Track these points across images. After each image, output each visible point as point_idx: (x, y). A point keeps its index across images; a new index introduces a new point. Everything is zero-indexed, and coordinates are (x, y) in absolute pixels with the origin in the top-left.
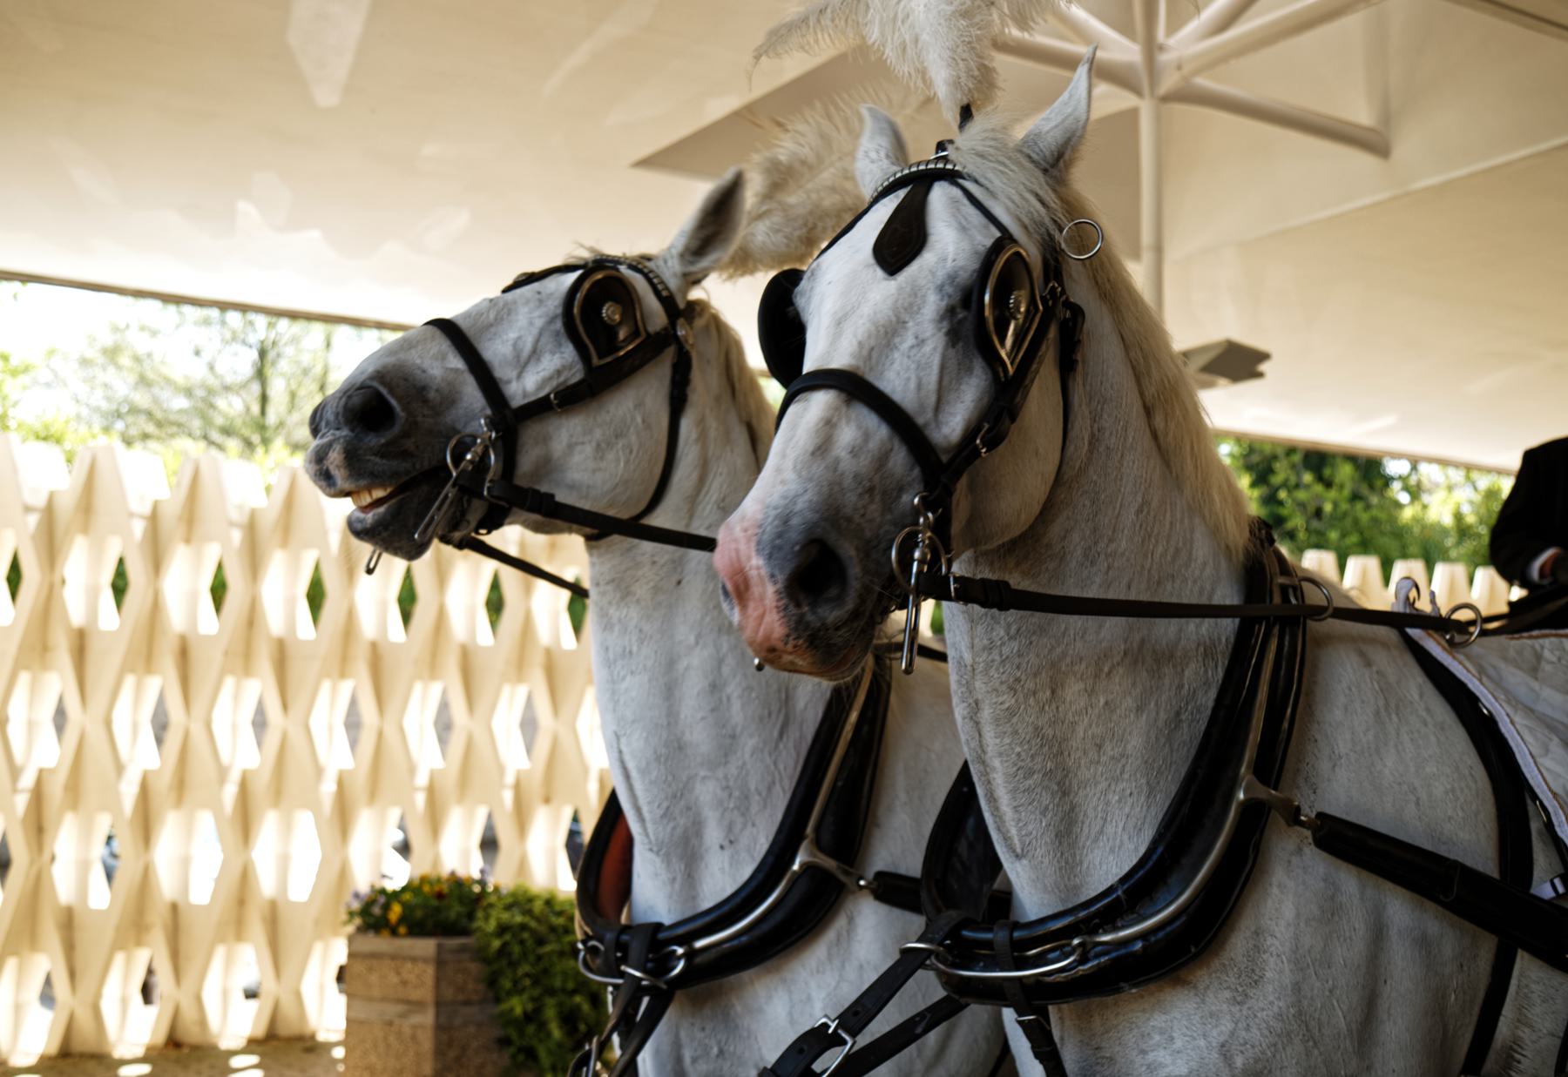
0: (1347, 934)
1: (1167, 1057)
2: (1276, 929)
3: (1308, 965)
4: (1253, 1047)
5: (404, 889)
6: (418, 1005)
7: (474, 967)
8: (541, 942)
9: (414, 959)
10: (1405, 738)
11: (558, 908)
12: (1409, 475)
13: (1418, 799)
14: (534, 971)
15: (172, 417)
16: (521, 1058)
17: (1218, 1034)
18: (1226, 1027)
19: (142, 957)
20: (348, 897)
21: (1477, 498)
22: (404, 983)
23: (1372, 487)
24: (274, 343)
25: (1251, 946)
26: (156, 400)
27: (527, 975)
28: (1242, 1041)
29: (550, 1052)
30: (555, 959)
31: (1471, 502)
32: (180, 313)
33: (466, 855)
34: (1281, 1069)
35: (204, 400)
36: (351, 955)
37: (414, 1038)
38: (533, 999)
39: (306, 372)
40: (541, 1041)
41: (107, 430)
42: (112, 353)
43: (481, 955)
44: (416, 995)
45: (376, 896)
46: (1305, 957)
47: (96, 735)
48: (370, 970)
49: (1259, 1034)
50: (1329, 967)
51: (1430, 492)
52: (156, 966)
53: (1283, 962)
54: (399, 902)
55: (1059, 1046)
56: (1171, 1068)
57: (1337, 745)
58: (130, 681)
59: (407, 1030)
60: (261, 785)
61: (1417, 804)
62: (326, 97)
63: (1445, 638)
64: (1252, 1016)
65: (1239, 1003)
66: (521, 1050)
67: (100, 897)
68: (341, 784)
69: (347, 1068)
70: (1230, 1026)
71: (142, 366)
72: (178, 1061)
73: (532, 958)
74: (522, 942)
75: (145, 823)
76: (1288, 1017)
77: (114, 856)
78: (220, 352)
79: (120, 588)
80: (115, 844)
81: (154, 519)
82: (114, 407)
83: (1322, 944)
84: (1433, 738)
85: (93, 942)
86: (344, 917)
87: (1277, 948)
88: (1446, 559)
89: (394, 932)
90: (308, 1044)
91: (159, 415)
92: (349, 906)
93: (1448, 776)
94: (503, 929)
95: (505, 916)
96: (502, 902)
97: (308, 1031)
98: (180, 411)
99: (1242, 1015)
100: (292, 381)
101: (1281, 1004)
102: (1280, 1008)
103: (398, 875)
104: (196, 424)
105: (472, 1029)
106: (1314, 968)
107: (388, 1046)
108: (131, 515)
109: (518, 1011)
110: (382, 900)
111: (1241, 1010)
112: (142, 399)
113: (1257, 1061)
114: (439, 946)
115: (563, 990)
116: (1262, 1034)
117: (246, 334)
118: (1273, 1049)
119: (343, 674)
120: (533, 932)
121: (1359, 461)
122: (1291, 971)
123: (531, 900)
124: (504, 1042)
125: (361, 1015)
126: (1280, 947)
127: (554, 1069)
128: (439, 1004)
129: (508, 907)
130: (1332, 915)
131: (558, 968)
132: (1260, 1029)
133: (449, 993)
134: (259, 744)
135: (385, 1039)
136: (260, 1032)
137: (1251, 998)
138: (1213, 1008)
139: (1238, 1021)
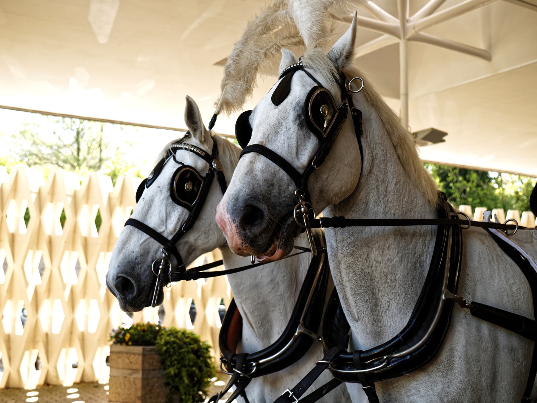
5: (131, 328)
6: (135, 371)
7: (156, 357)
8: (181, 348)
9: (134, 354)
11: (187, 336)
12: (498, 178)
15: (45, 156)
16: (173, 390)
19: (35, 353)
20: (110, 331)
21: (523, 186)
22: (131, 362)
23: (484, 182)
26: (39, 151)
27: (176, 360)
29: (184, 387)
30: (186, 354)
31: (520, 188)
32: (48, 118)
35: (56, 150)
36: (111, 352)
37: (134, 382)
38: (178, 369)
40: (180, 384)
41: (21, 161)
42: (23, 133)
43: (159, 352)
44: (135, 367)
47: (18, 272)
48: (119, 357)
51: (505, 184)
52: (40, 356)
54: (129, 333)
58: (31, 252)
59: (132, 380)
62: (103, 39)
66: (173, 387)
67: (20, 331)
71: (34, 137)
72: (48, 391)
73: (177, 354)
74: (174, 348)
75: (36, 304)
77: (25, 316)
79: (27, 219)
80: (25, 311)
81: (39, 193)
82: (24, 153)
85: (18, 346)
86: (109, 338)
88: (512, 208)
89: (127, 344)
90: (96, 385)
91: (40, 156)
92: (110, 334)
94: (167, 343)
95: (168, 338)
96: (167, 333)
97: (95, 380)
98: (48, 154)
100: (89, 143)
104: (54, 159)
105: (156, 379)
107: (125, 385)
108: (31, 192)
109: (172, 373)
110: (123, 332)
112: (34, 150)
114: (144, 349)
115: (189, 365)
119: (108, 250)
120: (178, 344)
121: (480, 172)
123: (177, 332)
124: (167, 384)
127: (185, 394)
128: (143, 370)
129: (169, 335)
131: (187, 357)
134: (78, 275)
135: (124, 382)
136: (78, 380)
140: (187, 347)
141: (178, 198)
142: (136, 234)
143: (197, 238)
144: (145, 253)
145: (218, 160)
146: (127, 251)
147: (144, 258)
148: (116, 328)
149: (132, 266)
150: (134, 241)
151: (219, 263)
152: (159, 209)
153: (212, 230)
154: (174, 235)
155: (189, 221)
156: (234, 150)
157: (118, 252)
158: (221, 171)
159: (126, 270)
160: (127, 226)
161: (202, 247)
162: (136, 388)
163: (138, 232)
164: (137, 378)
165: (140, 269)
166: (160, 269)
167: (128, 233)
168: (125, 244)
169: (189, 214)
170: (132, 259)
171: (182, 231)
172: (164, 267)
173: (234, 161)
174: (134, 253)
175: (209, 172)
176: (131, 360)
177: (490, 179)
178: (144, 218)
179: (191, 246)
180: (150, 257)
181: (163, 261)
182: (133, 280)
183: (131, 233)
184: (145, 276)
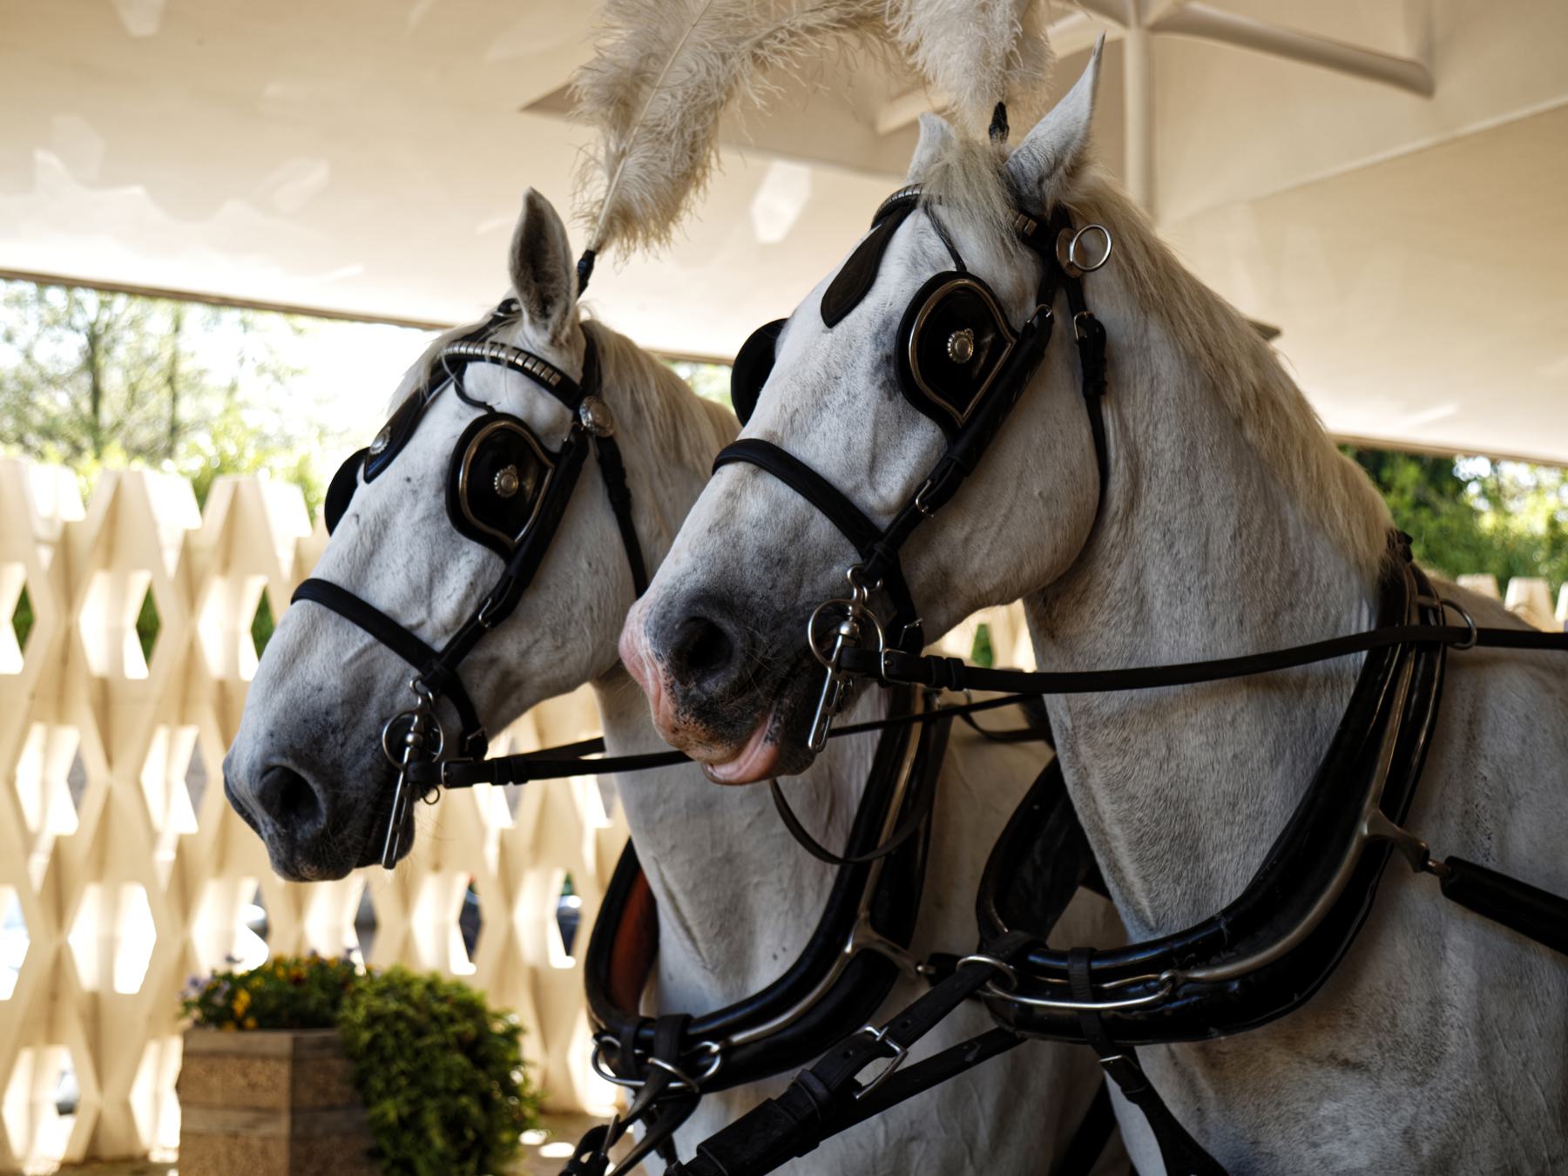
1: (1344, 1149)
2: (1456, 998)
3: (1496, 1036)
4: (1439, 1131)
6: (270, 1112)
7: (338, 1065)
8: (419, 1033)
9: (265, 1058)
11: (441, 993)
14: (410, 1068)
18: (1407, 1111)
22: (253, 1086)
25: (1427, 1019)
27: (403, 1073)
28: (1426, 1125)
30: (437, 1053)
33: (337, 932)
36: (187, 1055)
37: (264, 1152)
38: (410, 1102)
39: (150, 361)
43: (347, 1051)
44: (266, 1100)
45: (219, 982)
46: (1491, 1027)
49: (1444, 1117)
50: (1521, 1038)
53: (1466, 1035)
54: (247, 989)
55: (1192, 1129)
56: (1349, 1160)
57: (1514, 784)
59: (256, 1143)
65: (1419, 1084)
70: (1411, 1110)
73: (408, 1053)
74: (397, 1034)
76: (1476, 1096)
78: (38, 336)
83: (1511, 1013)
87: (1458, 1019)
92: (184, 995)
94: (373, 1019)
95: (377, 1004)
96: (374, 987)
99: (1424, 1097)
100: (132, 373)
101: (1467, 1083)
102: (1466, 1086)
103: (252, 956)
105: (336, 1140)
107: (232, 1163)
109: (392, 1116)
111: (1422, 1092)
113: (1444, 1147)
114: (296, 1041)
116: (1448, 1118)
117: (71, 316)
118: (1461, 1133)
120: (410, 1021)
122: (1476, 1044)
123: (408, 983)
125: (198, 1126)
126: (1461, 1017)
128: (295, 1110)
129: (381, 993)
130: (1521, 978)
131: (441, 1064)
132: (1444, 1111)
133: (307, 1097)
135: (229, 1154)
137: (1433, 1077)
138: (1391, 1091)
139: (1420, 1103)
140: (442, 1031)
141: (471, 515)
142: (330, 631)
143: (529, 647)
144: (360, 691)
145: (599, 398)
146: (298, 685)
147: (354, 713)
149: (316, 736)
150: (325, 651)
152: (407, 550)
153: (576, 623)
154: (451, 635)
155: (501, 594)
156: (646, 368)
157: (268, 689)
158: (607, 435)
159: (297, 747)
160: (298, 603)
163: (336, 624)
164: (273, 1138)
165: (342, 745)
168: (294, 661)
169: (503, 569)
170: (314, 712)
171: (479, 623)
172: (422, 738)
173: (647, 405)
174: (324, 694)
175: (572, 439)
177: (1461, 486)
178: (358, 579)
180: (375, 708)
181: (416, 719)
182: (315, 782)
183: (314, 625)
184: (357, 769)
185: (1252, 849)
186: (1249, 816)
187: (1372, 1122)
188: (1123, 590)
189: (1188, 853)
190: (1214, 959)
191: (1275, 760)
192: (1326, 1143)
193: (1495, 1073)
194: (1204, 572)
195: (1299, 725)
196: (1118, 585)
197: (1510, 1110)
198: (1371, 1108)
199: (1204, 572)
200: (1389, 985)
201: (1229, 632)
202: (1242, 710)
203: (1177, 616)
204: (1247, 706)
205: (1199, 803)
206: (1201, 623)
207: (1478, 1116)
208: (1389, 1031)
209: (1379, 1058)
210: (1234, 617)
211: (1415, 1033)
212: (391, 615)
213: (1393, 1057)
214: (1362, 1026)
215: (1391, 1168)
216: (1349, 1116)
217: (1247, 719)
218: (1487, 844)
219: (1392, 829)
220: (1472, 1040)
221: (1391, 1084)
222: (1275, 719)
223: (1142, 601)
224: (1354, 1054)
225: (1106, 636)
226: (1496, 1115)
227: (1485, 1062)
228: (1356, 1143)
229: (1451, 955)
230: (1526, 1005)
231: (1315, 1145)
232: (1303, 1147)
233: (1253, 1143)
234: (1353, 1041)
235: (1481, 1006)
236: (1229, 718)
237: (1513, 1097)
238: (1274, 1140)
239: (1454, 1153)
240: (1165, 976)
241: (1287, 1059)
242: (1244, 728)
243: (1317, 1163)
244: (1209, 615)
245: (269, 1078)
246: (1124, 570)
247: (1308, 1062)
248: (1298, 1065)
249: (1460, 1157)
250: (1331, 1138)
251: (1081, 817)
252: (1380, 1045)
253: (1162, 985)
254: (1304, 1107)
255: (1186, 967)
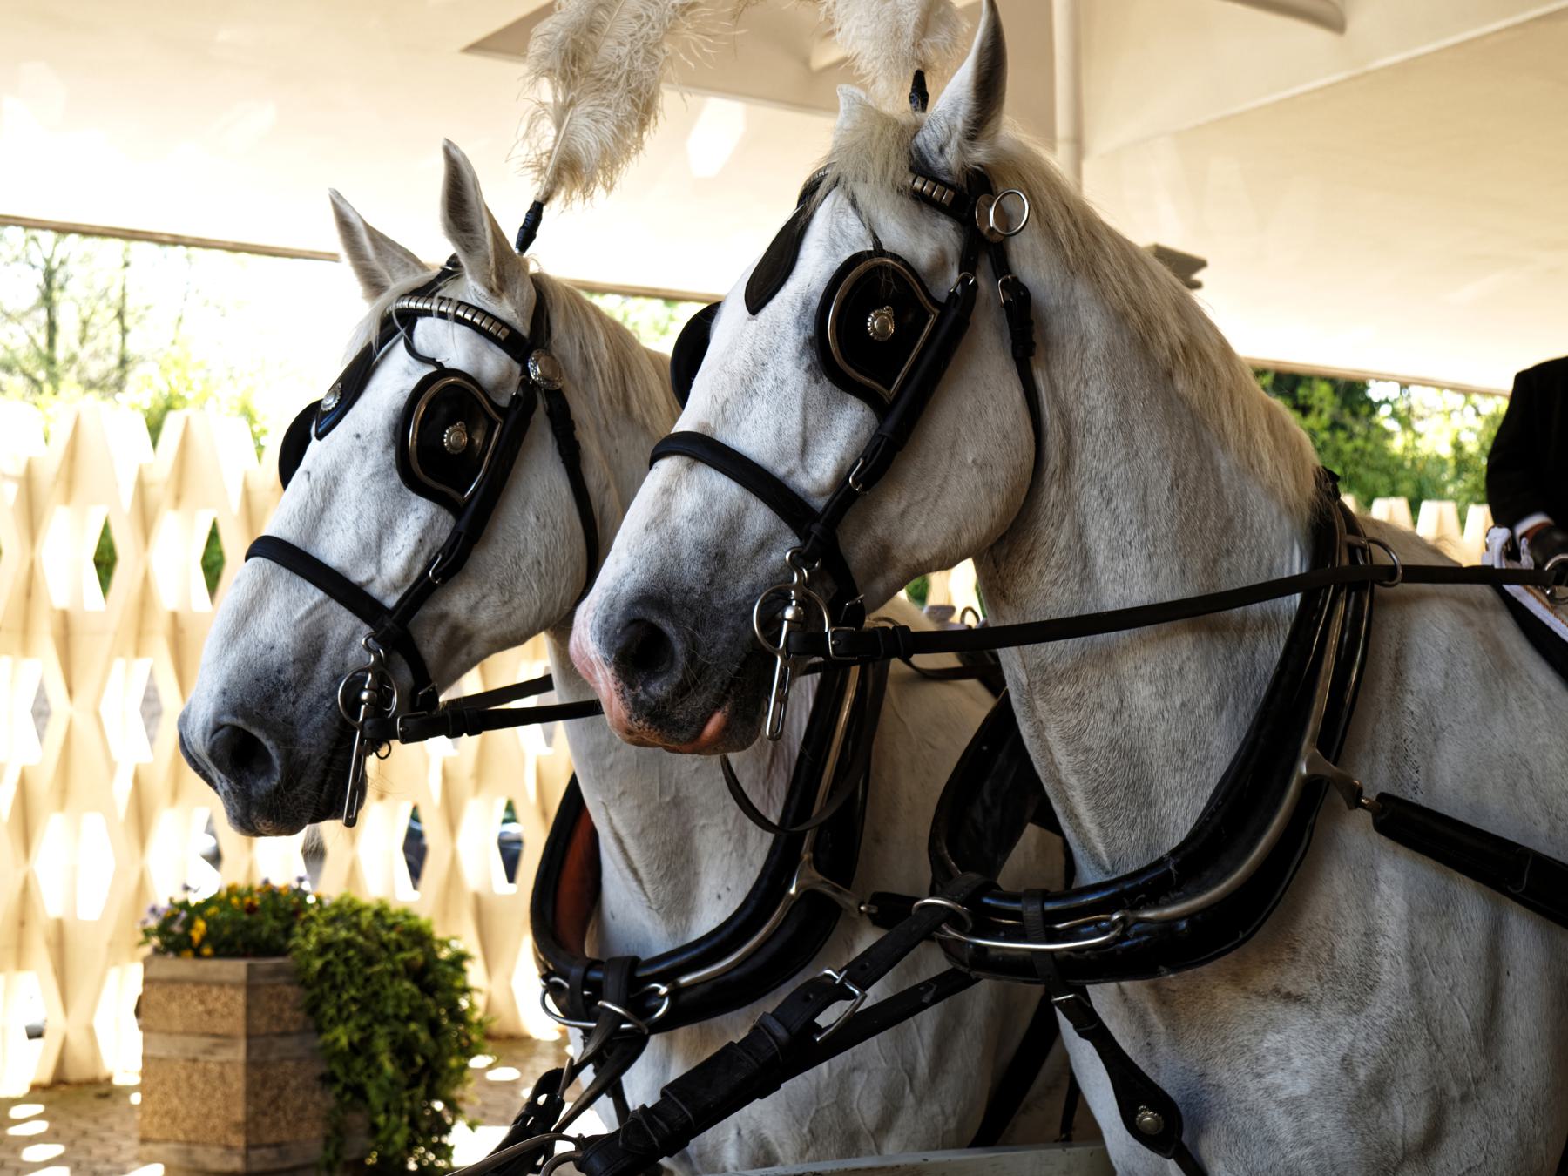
0: (1465, 925)
2: (1388, 928)
4: (1374, 1057)
5: (209, 902)
6: (226, 1038)
7: (291, 992)
8: (369, 961)
10: (1515, 706)
11: (390, 921)
13: (1531, 773)
16: (348, 1097)
17: (1337, 1049)
20: (145, 915)
22: (210, 1013)
24: (62, 263)
25: (1362, 950)
27: (354, 1000)
28: (1362, 1052)
29: (380, 1088)
30: (386, 980)
34: (1404, 1077)
36: (147, 981)
37: (222, 1076)
38: (362, 1029)
40: (370, 1077)
43: (300, 978)
44: (223, 1026)
48: (170, 997)
50: (1447, 963)
53: (1398, 964)
55: (1142, 1063)
56: (1288, 1091)
60: (43, 784)
61: (1530, 777)
63: (1545, 593)
64: (1370, 1024)
66: (346, 1088)
68: (137, 780)
69: (144, 1116)
70: (1349, 1038)
73: (359, 980)
74: (347, 961)
83: (1439, 941)
84: (1541, 707)
86: (141, 937)
89: (198, 954)
93: (1561, 747)
94: (325, 947)
96: (324, 914)
103: (206, 885)
105: (290, 1064)
106: (1432, 966)
107: (192, 1087)
109: (344, 1041)
110: (184, 915)
113: (1379, 1071)
114: (250, 967)
115: (396, 1016)
118: (1394, 1057)
119: (138, 653)
120: (360, 949)
123: (358, 912)
124: (328, 1079)
127: (387, 1110)
128: (249, 1036)
129: (331, 921)
130: (1447, 907)
131: (390, 992)
132: (1379, 1038)
133: (262, 1023)
134: (41, 737)
135: (189, 1077)
138: (1329, 1021)
139: (1357, 1031)
140: (390, 958)
142: (281, 587)
144: (311, 650)
147: (305, 671)
148: (163, 904)
149: (267, 694)
150: (277, 609)
151: (543, 684)
160: (251, 560)
161: (492, 632)
162: (226, 1096)
163: (287, 582)
164: (228, 1062)
165: (294, 703)
166: (363, 702)
167: (255, 584)
168: (247, 619)
174: (275, 652)
176: (211, 1007)
179: (455, 629)
183: (266, 584)
185: (1200, 793)
186: (1196, 762)
187: (1313, 1052)
188: (1068, 547)
189: (1142, 800)
190: (1163, 899)
191: (1220, 706)
192: (1268, 1074)
193: (1424, 999)
194: (1145, 525)
195: (1240, 669)
196: (1062, 543)
197: (1439, 1034)
198: (1311, 1038)
199: (1145, 525)
200: (1327, 918)
201: (1172, 583)
202: (1188, 658)
203: (1120, 570)
204: (1193, 654)
205: (1150, 751)
206: (1144, 575)
207: (1409, 1040)
208: (1327, 964)
209: (1318, 989)
210: (1177, 568)
211: (1352, 964)
212: (340, 571)
213: (1332, 988)
214: (1303, 960)
215: (1330, 1094)
216: (1292, 1047)
217: (1193, 667)
218: (1415, 777)
219: (1328, 769)
220: (1404, 967)
221: (1330, 1015)
222: (1219, 664)
223: (1086, 557)
224: (1296, 987)
225: (1054, 594)
226: (1426, 1039)
227: (1415, 988)
228: (1297, 1072)
229: (1383, 886)
230: (1452, 932)
231: (1259, 1076)
232: (1248, 1078)
233: (1201, 1076)
234: (1294, 974)
235: (1412, 934)
236: (1176, 667)
237: (1441, 1021)
238: (1221, 1073)
239: (1388, 1077)
240: (1116, 917)
241: (1233, 994)
242: (1191, 676)
243: (1261, 1092)
244: (1152, 568)
245: (226, 1005)
246: (1066, 527)
247: (1253, 996)
248: (1243, 1000)
249: (1393, 1080)
250: (1275, 1067)
251: (1037, 766)
252: (1319, 978)
253: (1114, 925)
254: (1249, 1040)
255: (1136, 907)
